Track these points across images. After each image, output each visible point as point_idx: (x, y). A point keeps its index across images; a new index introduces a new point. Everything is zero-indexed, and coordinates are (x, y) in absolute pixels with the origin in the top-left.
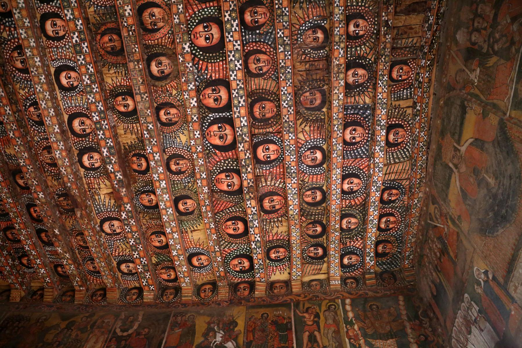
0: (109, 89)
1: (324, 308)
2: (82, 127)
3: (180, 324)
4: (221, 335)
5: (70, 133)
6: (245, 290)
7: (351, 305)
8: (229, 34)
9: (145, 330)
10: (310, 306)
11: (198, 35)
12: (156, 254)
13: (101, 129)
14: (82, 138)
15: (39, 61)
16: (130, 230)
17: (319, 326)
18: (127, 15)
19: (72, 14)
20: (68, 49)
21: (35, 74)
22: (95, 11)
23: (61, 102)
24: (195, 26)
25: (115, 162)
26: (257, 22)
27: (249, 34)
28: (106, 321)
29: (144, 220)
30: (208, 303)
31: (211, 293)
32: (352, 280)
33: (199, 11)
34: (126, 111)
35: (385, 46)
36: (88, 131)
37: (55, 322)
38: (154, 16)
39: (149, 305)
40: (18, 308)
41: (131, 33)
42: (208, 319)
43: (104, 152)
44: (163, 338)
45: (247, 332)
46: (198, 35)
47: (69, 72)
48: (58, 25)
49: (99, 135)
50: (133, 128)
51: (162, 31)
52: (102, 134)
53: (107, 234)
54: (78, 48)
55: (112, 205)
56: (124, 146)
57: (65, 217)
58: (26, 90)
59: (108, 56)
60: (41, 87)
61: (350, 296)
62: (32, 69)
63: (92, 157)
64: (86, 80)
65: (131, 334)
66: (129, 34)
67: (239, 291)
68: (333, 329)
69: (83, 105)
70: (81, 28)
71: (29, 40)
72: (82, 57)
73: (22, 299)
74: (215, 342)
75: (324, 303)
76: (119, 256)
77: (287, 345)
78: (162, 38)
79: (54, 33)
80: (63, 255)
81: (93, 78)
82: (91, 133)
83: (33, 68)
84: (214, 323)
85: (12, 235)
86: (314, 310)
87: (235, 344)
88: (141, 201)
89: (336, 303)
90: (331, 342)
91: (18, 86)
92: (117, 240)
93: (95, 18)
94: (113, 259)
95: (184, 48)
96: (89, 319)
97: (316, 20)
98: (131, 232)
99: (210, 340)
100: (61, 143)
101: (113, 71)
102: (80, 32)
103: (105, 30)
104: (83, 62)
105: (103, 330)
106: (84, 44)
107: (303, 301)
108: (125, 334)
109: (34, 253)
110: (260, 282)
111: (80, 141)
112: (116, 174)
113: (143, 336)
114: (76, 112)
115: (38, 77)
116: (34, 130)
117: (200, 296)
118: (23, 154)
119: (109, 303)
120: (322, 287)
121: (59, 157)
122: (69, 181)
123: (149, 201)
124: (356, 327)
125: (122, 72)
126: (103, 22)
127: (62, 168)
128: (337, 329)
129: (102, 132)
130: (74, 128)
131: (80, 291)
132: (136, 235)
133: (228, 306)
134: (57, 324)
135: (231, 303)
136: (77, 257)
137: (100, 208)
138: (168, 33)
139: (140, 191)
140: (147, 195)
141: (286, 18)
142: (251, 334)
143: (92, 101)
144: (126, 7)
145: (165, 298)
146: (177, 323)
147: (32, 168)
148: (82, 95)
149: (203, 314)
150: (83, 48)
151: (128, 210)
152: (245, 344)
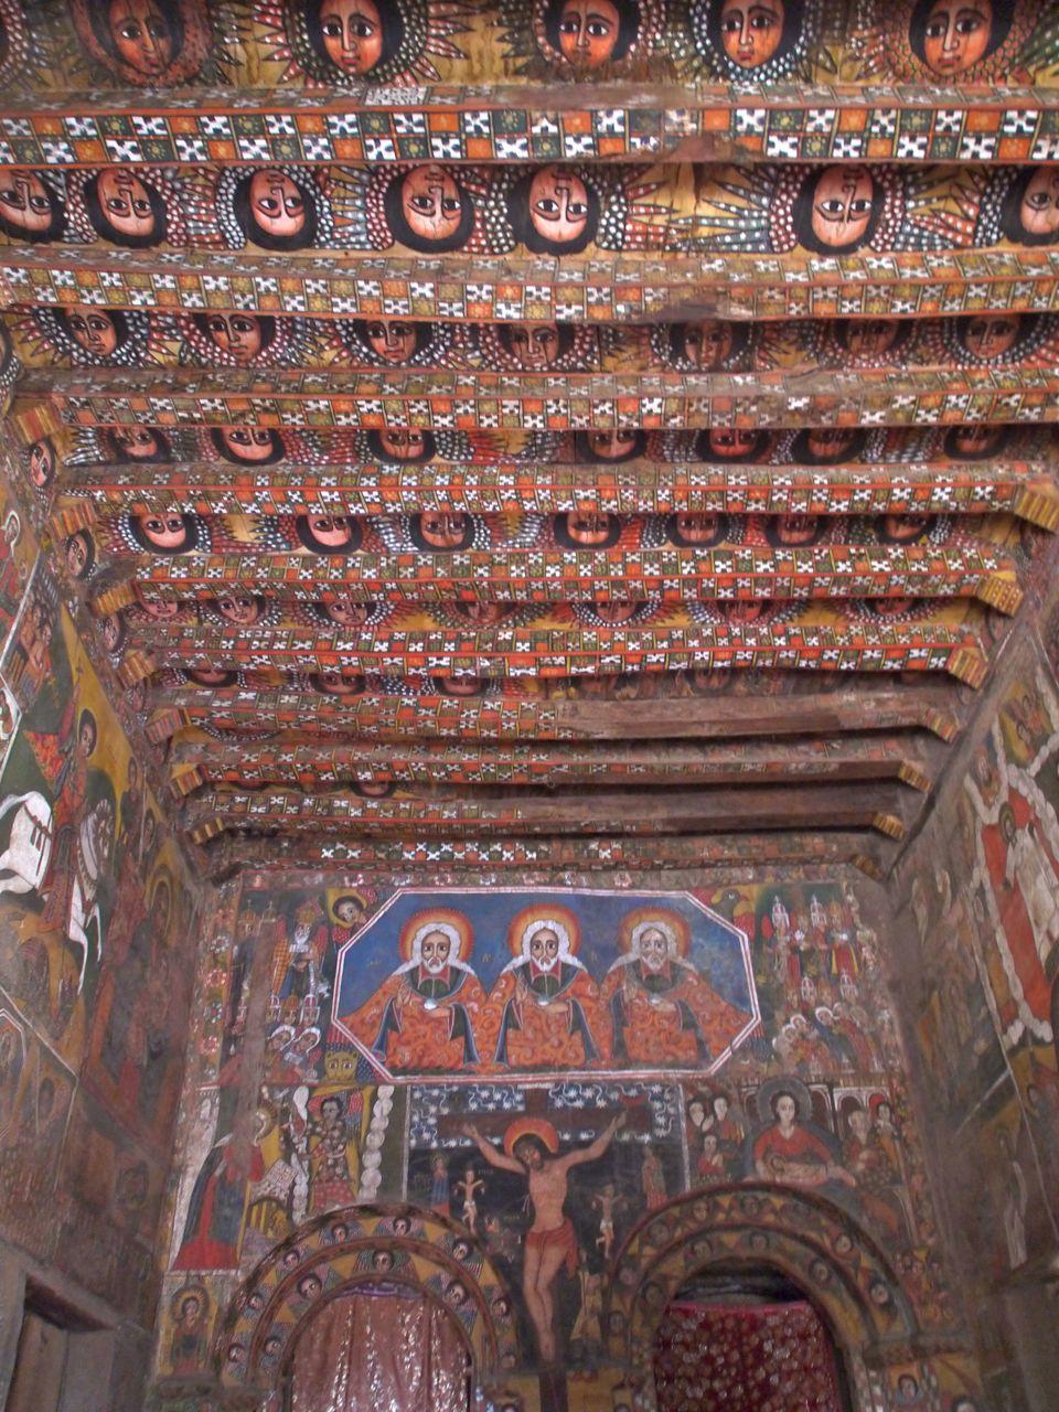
0: (301, 79)
2: (438, 207)
5: (457, 256)
12: (1028, 60)
13: (424, 141)
14: (474, 219)
15: (215, 278)
16: (856, 142)
19: (56, 143)
20: (184, 185)
21: (253, 301)
22: (51, 66)
23: (353, 254)
25: (555, 122)
29: (846, 69)
34: (378, 31)
36: (451, 193)
40: (1037, 605)
43: (513, 155)
47: (256, 203)
48: (117, 196)
49: (446, 154)
50: (443, 18)
52: (445, 141)
53: (866, 238)
54: (156, 150)
55: (747, 184)
56: (517, 72)
57: (763, 359)
58: (323, 341)
59: (188, 55)
60: (293, 297)
62: (240, 306)
63: (548, 204)
64: (255, 150)
69: (362, 184)
70: (91, 126)
71: (159, 290)
72: (181, 143)
73: (1022, 583)
76: (978, 221)
79: (143, 213)
80: (897, 411)
81: (248, 125)
82: (457, 183)
83: (237, 301)
85: (799, 530)
88: (756, 59)
91: (313, 359)
92: (904, 209)
93: (71, 73)
94: (984, 250)
98: (866, 141)
100: (469, 288)
101: (239, 47)
102: (105, 132)
103: (102, 43)
104: (198, 144)
106: (139, 127)
109: (865, 495)
111: (484, 229)
112: (602, 128)
114: (386, 213)
115: (259, 294)
116: (445, 356)
118: (506, 411)
121: (518, 310)
122: (610, 304)
123: (760, 26)
125: (239, 17)
126: (77, 45)
127: (560, 312)
129: (436, 142)
130: (439, 236)
132: (884, 121)
136: (935, 373)
137: (749, 231)
139: (710, 56)
140: (731, 28)
143: (326, 148)
147: (557, 402)
148: (328, 179)
150: (151, 132)
151: (761, 121)
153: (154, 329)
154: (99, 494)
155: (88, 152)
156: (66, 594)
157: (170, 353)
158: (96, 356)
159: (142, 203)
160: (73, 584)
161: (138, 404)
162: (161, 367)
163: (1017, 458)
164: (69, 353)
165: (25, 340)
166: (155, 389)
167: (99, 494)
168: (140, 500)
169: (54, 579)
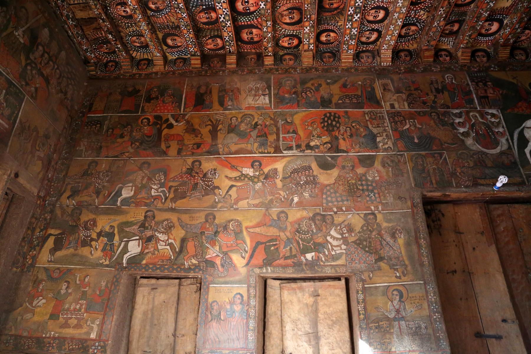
8: (226, 14)
11: (254, 5)
18: (308, 28)
22: (338, 22)
24: (257, 10)
26: (205, 13)
27: (211, 4)
33: (253, 20)
35: (96, 7)
38: (290, 18)
41: (309, 17)
46: (254, 5)
51: (285, 8)
66: (310, 16)
72: (357, 4)
78: (286, 3)
95: (264, 5)
97: (160, 15)
102: (351, 20)
103: (334, 11)
126: (334, 16)
138: (280, 7)
141: (183, 24)
144: (308, 31)
153: (414, 16)
154: (462, 46)
155: (355, 25)
156: (488, 69)
157: (424, 14)
158: (418, 32)
159: (376, 11)
160: (488, 64)
161: (434, 30)
162: (427, 17)
164: (415, 38)
165: (408, 46)
166: (432, 22)
167: (462, 46)
168: (470, 36)
169: (479, 71)
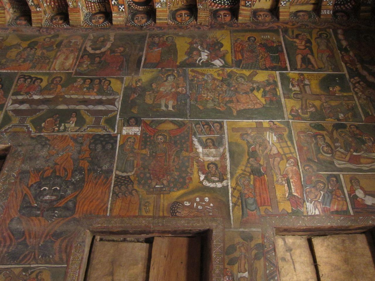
1: (314, 36)
3: (158, 44)
4: (206, 54)
6: (226, 16)
7: (343, 35)
9: (120, 48)
10: (300, 33)
17: (312, 50)
28: (73, 41)
30: (187, 27)
31: (189, 17)
32: (342, 14)
37: (15, 42)
39: (119, 27)
42: (190, 40)
44: (142, 56)
45: (235, 52)
61: (342, 27)
65: (105, 52)
67: (219, 17)
68: (327, 54)
74: (200, 60)
75: (314, 32)
77: (280, 64)
84: (196, 43)
86: (304, 37)
87: (223, 62)
89: (328, 32)
90: (326, 65)
96: (53, 40)
99: (195, 58)
105: (71, 49)
107: (291, 28)
108: (98, 52)
110: (245, 6)
113: (119, 54)
117: (176, 20)
119: (73, 26)
120: (310, 17)
124: (351, 54)
128: (331, 54)
131: (37, 12)
133: (209, 29)
134: (17, 44)
135: (212, 27)
142: (239, 53)
145: (136, 21)
146: (154, 43)
149: (183, 36)
152: (234, 62)
163: (11, 3)
